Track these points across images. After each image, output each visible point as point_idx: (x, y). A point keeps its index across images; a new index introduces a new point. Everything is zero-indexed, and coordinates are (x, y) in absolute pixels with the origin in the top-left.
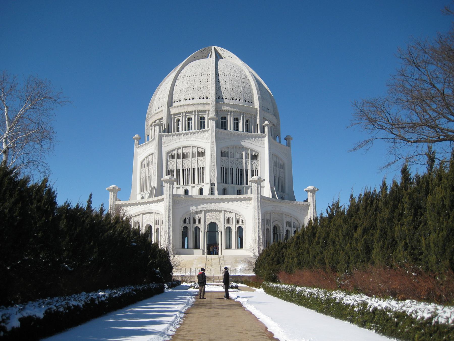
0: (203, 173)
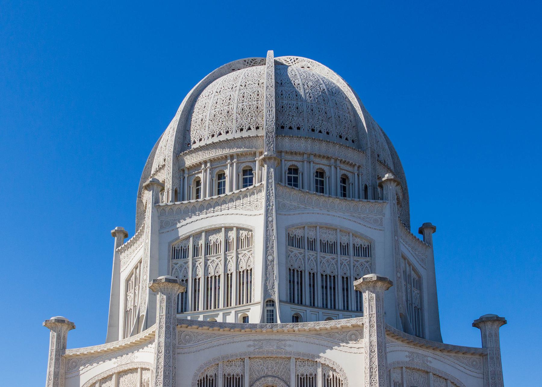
0: (249, 283)
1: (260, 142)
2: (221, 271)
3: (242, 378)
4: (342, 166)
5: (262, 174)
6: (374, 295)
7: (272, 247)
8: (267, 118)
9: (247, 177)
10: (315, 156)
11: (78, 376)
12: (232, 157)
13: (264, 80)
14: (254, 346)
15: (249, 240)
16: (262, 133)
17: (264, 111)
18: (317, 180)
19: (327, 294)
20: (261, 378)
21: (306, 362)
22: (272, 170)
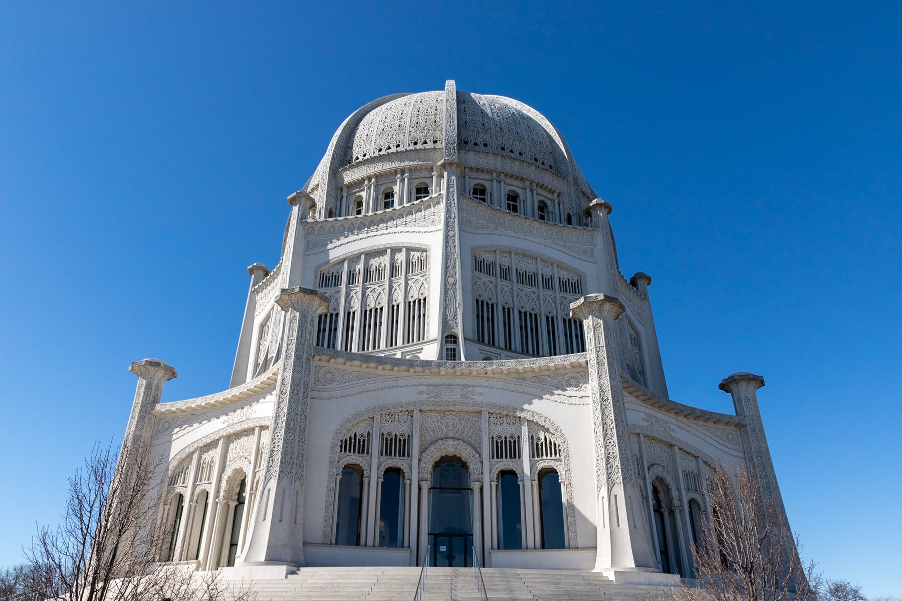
0: (422, 316)
1: (438, 154)
2: (384, 302)
3: (409, 440)
4: (539, 191)
5: (442, 187)
6: (601, 321)
9: (422, 191)
11: (170, 442)
12: (403, 172)
13: (443, 107)
15: (423, 263)
17: (444, 125)
18: (509, 205)
19: (527, 336)
20: (437, 441)
21: (505, 419)
22: (454, 178)
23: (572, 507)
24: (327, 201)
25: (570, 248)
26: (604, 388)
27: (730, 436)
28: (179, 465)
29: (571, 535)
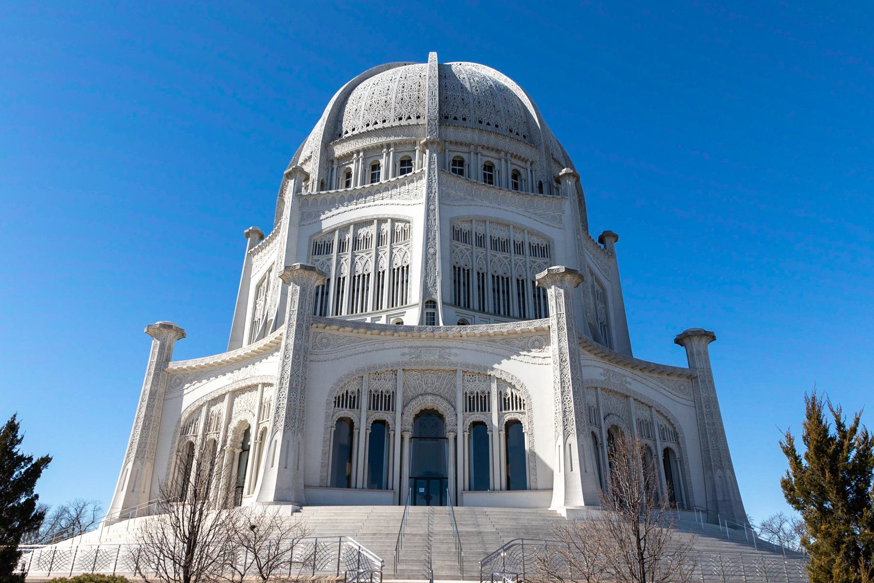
0: (405, 282)
1: (420, 130)
4: (513, 160)
5: (424, 162)
7: (434, 239)
8: (429, 106)
9: (405, 165)
10: (483, 147)
11: (182, 396)
12: (388, 146)
14: (410, 354)
15: (406, 233)
16: (423, 121)
17: (427, 101)
18: (485, 174)
20: (418, 396)
23: (534, 454)
24: (319, 173)
25: (540, 215)
26: (563, 350)
27: (682, 387)
28: (190, 416)
29: (532, 478)
